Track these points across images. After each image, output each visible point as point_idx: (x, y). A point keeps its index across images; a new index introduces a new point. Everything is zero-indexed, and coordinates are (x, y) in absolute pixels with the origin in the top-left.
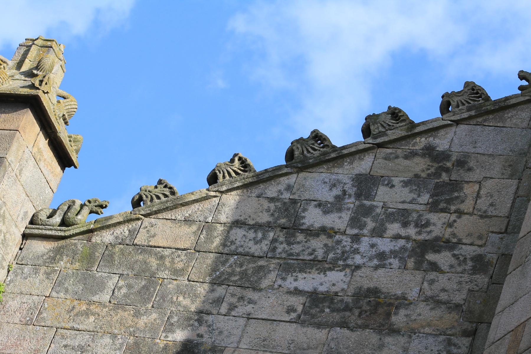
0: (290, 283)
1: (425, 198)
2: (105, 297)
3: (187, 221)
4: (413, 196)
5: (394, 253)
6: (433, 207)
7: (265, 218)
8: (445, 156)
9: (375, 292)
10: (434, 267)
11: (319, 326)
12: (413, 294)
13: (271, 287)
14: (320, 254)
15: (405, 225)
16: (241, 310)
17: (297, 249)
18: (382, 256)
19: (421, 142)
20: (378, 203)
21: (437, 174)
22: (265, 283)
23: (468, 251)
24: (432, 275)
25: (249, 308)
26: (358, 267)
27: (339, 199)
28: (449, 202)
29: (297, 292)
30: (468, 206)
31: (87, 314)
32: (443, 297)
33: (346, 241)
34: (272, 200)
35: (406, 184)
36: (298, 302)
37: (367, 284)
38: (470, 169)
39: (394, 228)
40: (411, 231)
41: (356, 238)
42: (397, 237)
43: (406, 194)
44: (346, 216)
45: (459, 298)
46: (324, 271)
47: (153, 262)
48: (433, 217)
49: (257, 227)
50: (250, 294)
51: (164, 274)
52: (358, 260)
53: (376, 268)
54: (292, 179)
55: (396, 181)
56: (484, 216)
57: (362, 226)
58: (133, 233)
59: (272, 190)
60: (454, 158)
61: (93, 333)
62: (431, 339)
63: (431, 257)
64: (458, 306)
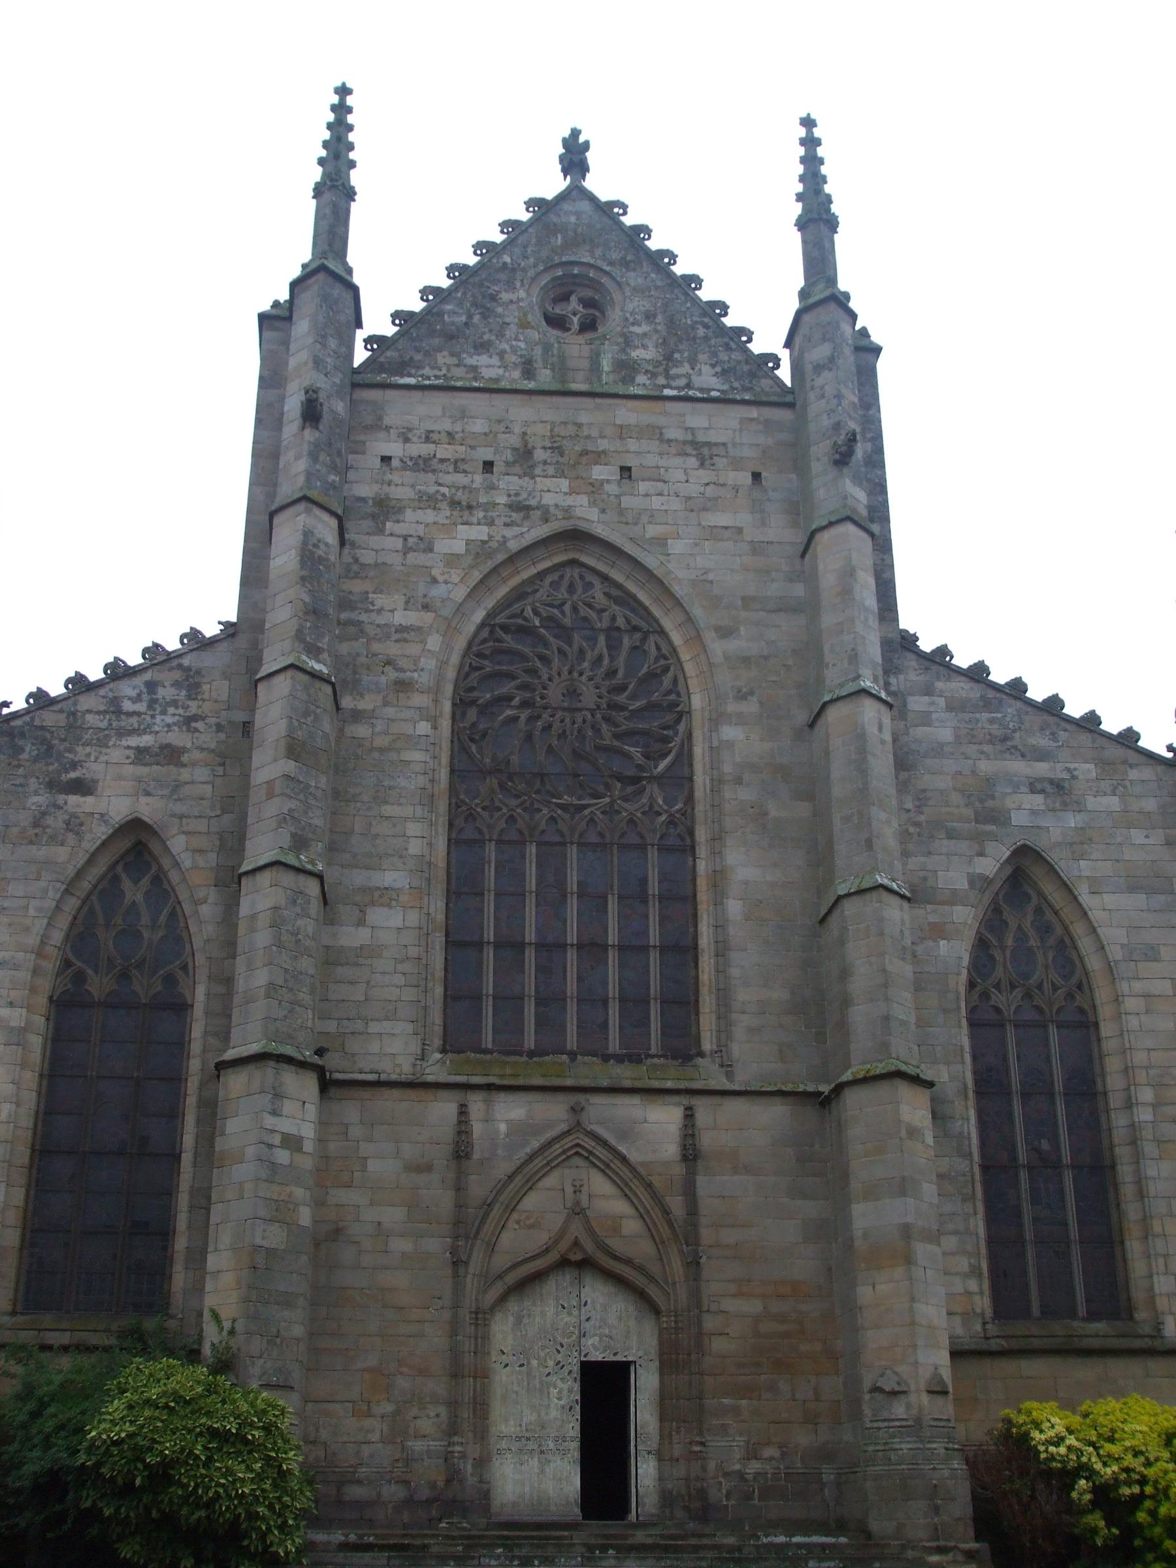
0: (124, 743)
1: (184, 693)
2: (24, 756)
3: (61, 711)
4: (177, 692)
5: (174, 724)
6: (189, 697)
7: (102, 708)
8: (189, 669)
9: (169, 745)
10: (196, 730)
11: (145, 765)
12: (189, 745)
13: (114, 745)
14: (136, 726)
15: (177, 708)
16: (103, 758)
17: (123, 724)
18: (169, 726)
19: (175, 663)
20: (159, 696)
21: (187, 680)
22: (111, 743)
23: (212, 721)
24: (197, 734)
25: (106, 757)
26: (157, 732)
27: (139, 695)
28: (196, 694)
29: (128, 747)
30: (206, 696)
31: (19, 766)
32: (205, 746)
33: (148, 718)
34: (103, 697)
35: (172, 685)
36: (131, 753)
37: (165, 741)
38: (203, 676)
39: (171, 710)
40: (181, 711)
41: (153, 717)
42: (174, 715)
43: (173, 691)
44: (145, 704)
45: (213, 746)
46: (139, 735)
47: (48, 736)
48: (190, 703)
49: (98, 713)
50: (104, 750)
51: (56, 742)
52: (157, 728)
53: (167, 732)
54: (111, 685)
55: (166, 684)
56: (216, 701)
57: (155, 710)
58: (33, 719)
59: (102, 692)
60: (194, 670)
61: (25, 777)
62: (204, 769)
63: (194, 725)
64: (213, 751)
